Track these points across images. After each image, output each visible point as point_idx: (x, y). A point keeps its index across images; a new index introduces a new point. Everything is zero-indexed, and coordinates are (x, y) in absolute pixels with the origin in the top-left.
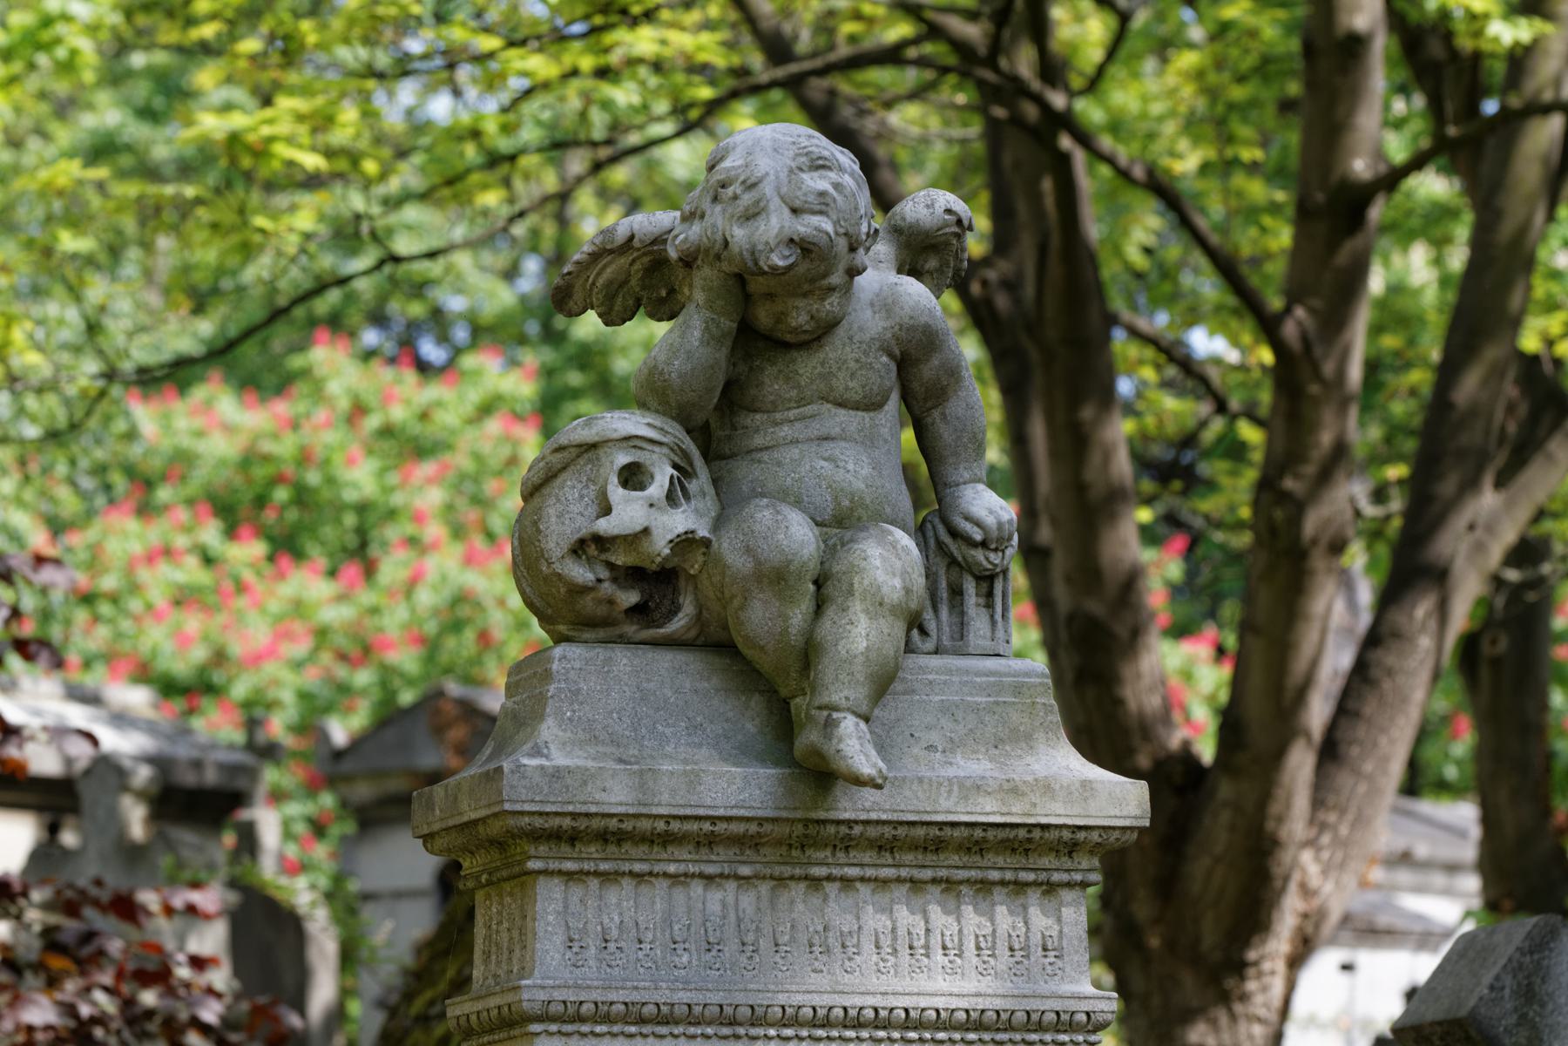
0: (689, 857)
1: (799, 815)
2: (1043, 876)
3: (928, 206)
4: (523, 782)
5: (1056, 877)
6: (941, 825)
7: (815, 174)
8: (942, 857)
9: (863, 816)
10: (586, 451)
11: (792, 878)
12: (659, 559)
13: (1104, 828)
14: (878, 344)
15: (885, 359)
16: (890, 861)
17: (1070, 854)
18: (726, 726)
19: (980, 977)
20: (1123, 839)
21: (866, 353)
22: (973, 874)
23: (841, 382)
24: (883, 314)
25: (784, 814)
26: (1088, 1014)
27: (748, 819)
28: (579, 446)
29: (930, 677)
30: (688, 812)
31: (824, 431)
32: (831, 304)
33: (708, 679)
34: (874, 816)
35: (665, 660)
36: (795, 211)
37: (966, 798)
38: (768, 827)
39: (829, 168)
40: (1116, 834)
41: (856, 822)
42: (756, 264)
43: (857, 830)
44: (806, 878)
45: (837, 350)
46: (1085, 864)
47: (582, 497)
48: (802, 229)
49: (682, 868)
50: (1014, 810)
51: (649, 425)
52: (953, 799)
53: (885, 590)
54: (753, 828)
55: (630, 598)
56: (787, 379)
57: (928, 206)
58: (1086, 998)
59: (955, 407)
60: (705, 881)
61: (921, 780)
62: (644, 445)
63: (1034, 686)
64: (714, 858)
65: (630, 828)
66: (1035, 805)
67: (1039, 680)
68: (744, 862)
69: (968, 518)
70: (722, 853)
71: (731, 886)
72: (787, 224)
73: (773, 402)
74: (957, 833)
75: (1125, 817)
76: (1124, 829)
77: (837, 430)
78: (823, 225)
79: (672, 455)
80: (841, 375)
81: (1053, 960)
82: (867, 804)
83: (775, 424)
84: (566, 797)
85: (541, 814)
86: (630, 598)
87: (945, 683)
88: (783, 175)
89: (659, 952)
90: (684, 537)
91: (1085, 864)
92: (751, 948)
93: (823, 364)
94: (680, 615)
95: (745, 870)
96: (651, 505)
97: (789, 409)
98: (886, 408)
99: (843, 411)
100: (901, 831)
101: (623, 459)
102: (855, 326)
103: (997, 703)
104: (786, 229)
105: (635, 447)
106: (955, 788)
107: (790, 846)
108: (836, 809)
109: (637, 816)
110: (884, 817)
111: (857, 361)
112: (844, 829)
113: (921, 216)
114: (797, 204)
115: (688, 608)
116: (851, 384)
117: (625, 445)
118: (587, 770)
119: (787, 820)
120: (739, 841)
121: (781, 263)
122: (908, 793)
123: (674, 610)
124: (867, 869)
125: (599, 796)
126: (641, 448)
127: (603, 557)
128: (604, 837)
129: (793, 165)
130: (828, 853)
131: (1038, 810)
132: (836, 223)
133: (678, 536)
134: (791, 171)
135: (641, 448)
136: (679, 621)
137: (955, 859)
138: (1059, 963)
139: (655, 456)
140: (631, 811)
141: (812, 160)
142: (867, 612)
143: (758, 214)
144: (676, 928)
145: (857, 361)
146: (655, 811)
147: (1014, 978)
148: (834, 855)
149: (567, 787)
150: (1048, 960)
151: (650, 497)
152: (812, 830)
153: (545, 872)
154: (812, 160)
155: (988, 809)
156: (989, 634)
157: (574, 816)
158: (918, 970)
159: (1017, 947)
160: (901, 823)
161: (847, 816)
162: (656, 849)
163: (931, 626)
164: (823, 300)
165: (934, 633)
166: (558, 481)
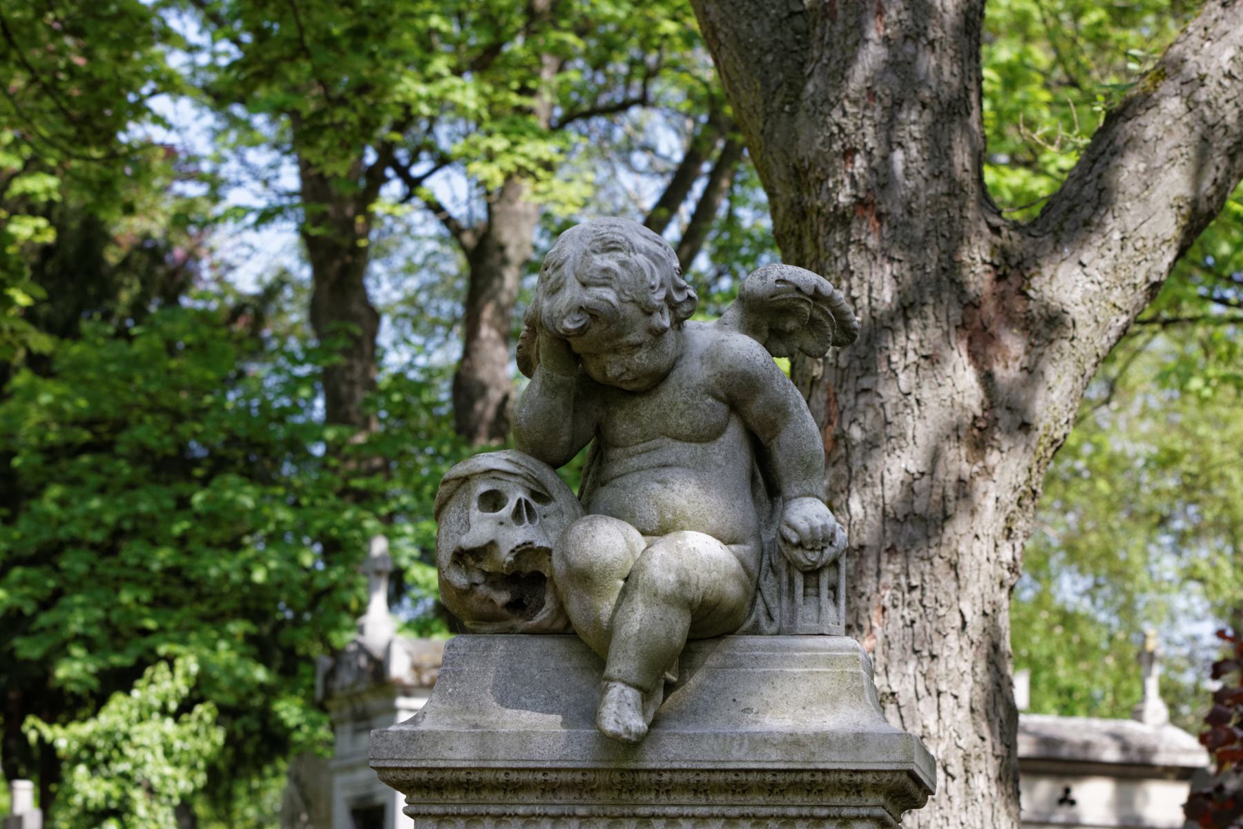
0: (536, 801)
1: (613, 765)
2: (834, 812)
3: (761, 278)
4: (385, 744)
5: (845, 812)
6: (737, 771)
7: (606, 255)
8: (749, 797)
9: (667, 766)
10: (463, 483)
11: (623, 816)
13: (877, 771)
14: (703, 389)
15: (710, 400)
16: (704, 801)
17: (859, 792)
18: (578, 696)
20: (895, 780)
21: (692, 397)
22: (775, 810)
23: (673, 420)
24: (709, 365)
25: (601, 765)
27: (574, 770)
28: (457, 479)
29: (757, 653)
30: (521, 765)
31: (663, 460)
32: (640, 358)
33: (570, 660)
34: (676, 765)
35: (537, 645)
36: (584, 285)
37: (755, 749)
38: (590, 777)
39: (620, 250)
40: (888, 776)
41: (665, 771)
42: (554, 325)
43: (666, 777)
44: (635, 816)
45: (670, 395)
46: (871, 801)
47: (459, 519)
48: (587, 299)
49: (529, 810)
50: (795, 758)
51: (507, 460)
52: (744, 750)
53: (659, 583)
54: (578, 777)
55: (502, 598)
56: (632, 420)
57: (761, 278)
59: (786, 437)
61: (716, 736)
62: (501, 476)
63: (846, 658)
64: (556, 801)
65: (477, 779)
66: (813, 754)
67: (849, 653)
68: (582, 805)
69: (789, 525)
70: (564, 797)
72: (577, 295)
73: (624, 439)
74: (751, 778)
75: (892, 763)
76: (893, 771)
77: (673, 458)
78: (604, 295)
79: (527, 484)
80: (673, 415)
82: (670, 756)
83: (630, 456)
84: (419, 755)
85: (403, 769)
86: (502, 598)
87: (769, 657)
88: (579, 258)
91: (871, 801)
93: (659, 406)
95: (581, 811)
96: (501, 523)
97: (637, 444)
98: (721, 439)
99: (678, 444)
100: (703, 777)
101: (483, 487)
102: (685, 375)
103: (811, 673)
104: (576, 300)
106: (746, 741)
107: (620, 791)
108: (644, 760)
109: (482, 769)
110: (685, 766)
111: (685, 403)
112: (654, 777)
113: (755, 286)
114: (585, 278)
115: (549, 603)
116: (681, 422)
118: (437, 733)
119: (607, 770)
120: (571, 787)
121: (571, 326)
122: (705, 746)
123: (542, 604)
125: (450, 754)
127: (478, 566)
128: (495, 787)
129: (588, 249)
130: (653, 795)
131: (817, 758)
132: (620, 292)
134: (586, 254)
137: (760, 799)
139: (510, 485)
140: (473, 765)
141: (605, 244)
142: (644, 601)
143: (558, 289)
145: (685, 403)
146: (493, 765)
148: (657, 795)
149: (421, 748)
151: (500, 517)
152: (628, 778)
154: (605, 244)
155: (774, 757)
156: (815, 618)
157: (430, 770)
160: (703, 771)
161: (653, 766)
162: (509, 795)
163: (776, 613)
164: (632, 355)
165: (777, 619)
166: (447, 508)
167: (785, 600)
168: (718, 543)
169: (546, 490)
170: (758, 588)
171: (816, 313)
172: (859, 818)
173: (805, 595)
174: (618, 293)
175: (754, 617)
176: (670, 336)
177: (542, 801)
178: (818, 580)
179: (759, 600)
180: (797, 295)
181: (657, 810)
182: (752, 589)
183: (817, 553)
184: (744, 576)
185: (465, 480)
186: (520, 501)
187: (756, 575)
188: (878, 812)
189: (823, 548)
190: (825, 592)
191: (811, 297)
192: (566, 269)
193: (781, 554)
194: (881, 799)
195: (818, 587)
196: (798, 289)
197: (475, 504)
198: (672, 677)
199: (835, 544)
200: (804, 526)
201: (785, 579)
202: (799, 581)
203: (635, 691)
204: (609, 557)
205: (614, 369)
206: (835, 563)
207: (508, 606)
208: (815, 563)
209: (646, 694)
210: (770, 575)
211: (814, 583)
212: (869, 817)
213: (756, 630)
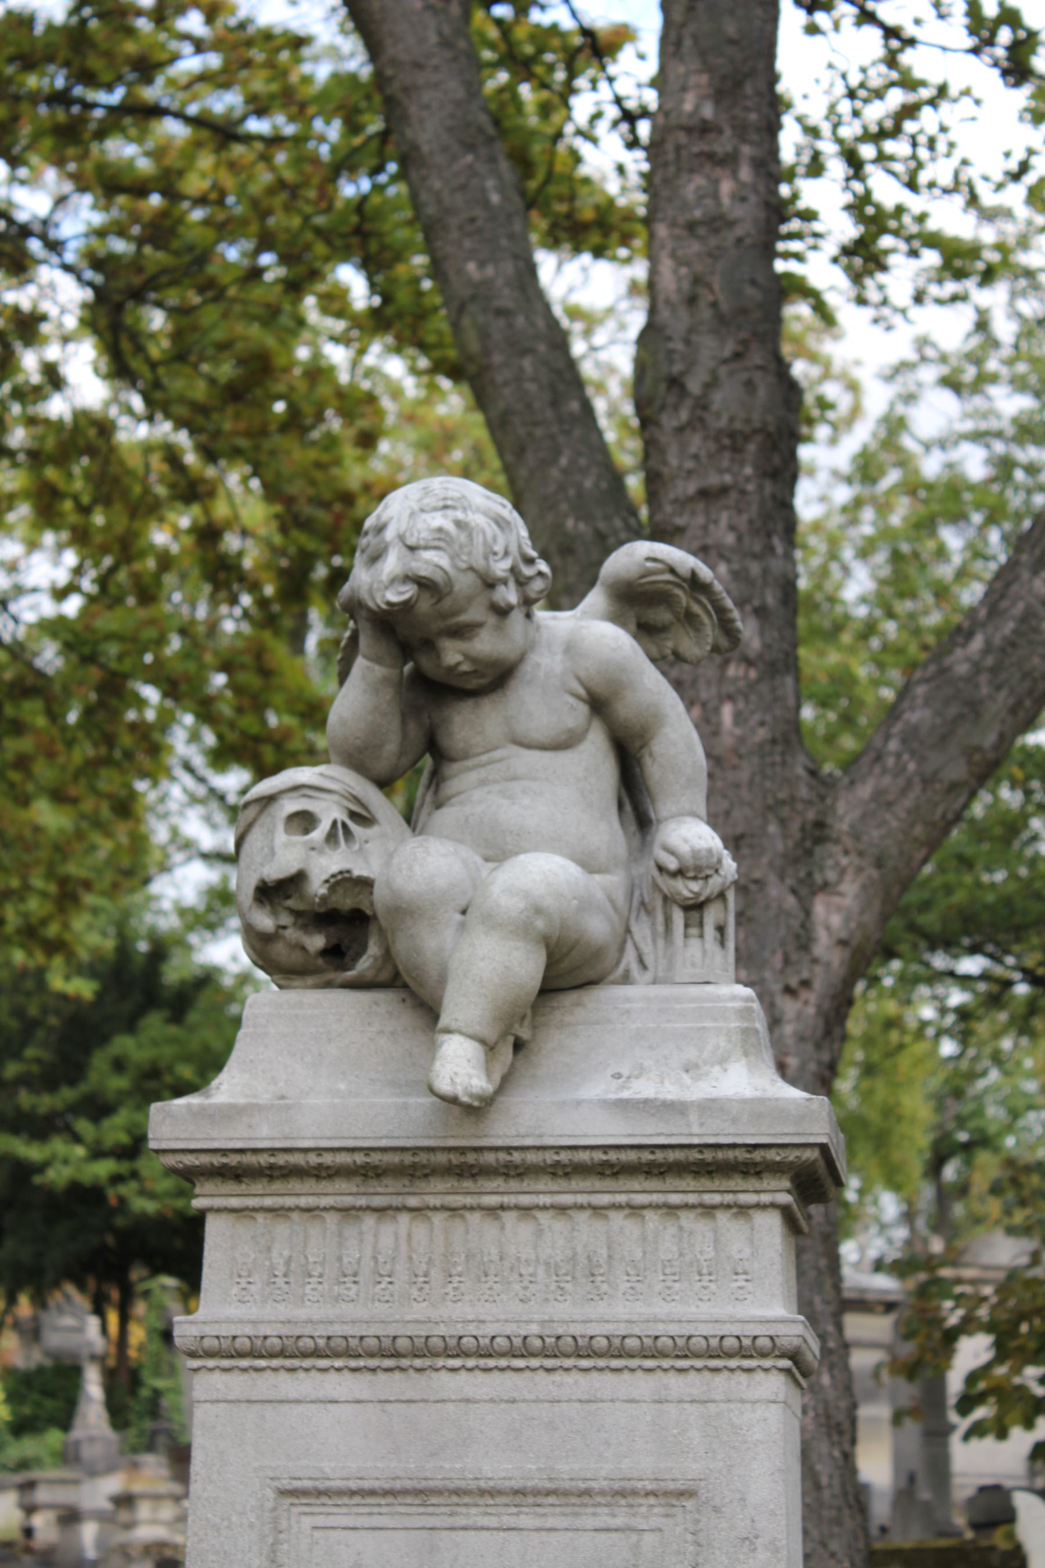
12: (317, 900)
19: (663, 1303)
26: (771, 1338)
27: (403, 1149)
29: (627, 1006)
39: (454, 508)
54: (408, 1159)
55: (317, 942)
58: (768, 1321)
60: (376, 1215)
71: (404, 1218)
81: (744, 1284)
86: (317, 942)
89: (326, 1286)
90: (339, 877)
92: (422, 1279)
94: (365, 957)
96: (313, 849)
101: (291, 805)
105: (304, 796)
112: (503, 1156)
114: (411, 541)
115: (373, 949)
117: (294, 794)
124: (541, 1196)
126: (309, 797)
133: (333, 876)
134: (412, 514)
138: (713, 1286)
144: (345, 1260)
147: (700, 1303)
151: (311, 841)
153: (219, 1210)
158: (597, 1298)
159: (705, 1271)
161: (499, 1142)
163: (649, 960)
167: (661, 943)
168: (579, 869)
170: (628, 931)
171: (696, 608)
172: (759, 1206)
173: (686, 936)
174: (452, 558)
176: (517, 617)
177: (362, 1190)
179: (629, 945)
180: (668, 577)
181: (506, 1199)
182: (621, 930)
183: (701, 882)
184: (611, 912)
185: (269, 800)
186: (334, 823)
187: (626, 912)
188: (785, 1198)
189: (707, 877)
190: (710, 931)
191: (684, 580)
192: (389, 534)
193: (656, 887)
195: (701, 925)
196: (672, 571)
197: (280, 827)
198: (525, 1033)
199: (722, 872)
200: (684, 849)
201: (660, 918)
202: (678, 917)
203: (476, 1044)
205: (452, 653)
206: (722, 896)
207: (325, 953)
208: (697, 894)
209: (490, 1048)
210: (643, 913)
212: (773, 1205)
213: (626, 979)
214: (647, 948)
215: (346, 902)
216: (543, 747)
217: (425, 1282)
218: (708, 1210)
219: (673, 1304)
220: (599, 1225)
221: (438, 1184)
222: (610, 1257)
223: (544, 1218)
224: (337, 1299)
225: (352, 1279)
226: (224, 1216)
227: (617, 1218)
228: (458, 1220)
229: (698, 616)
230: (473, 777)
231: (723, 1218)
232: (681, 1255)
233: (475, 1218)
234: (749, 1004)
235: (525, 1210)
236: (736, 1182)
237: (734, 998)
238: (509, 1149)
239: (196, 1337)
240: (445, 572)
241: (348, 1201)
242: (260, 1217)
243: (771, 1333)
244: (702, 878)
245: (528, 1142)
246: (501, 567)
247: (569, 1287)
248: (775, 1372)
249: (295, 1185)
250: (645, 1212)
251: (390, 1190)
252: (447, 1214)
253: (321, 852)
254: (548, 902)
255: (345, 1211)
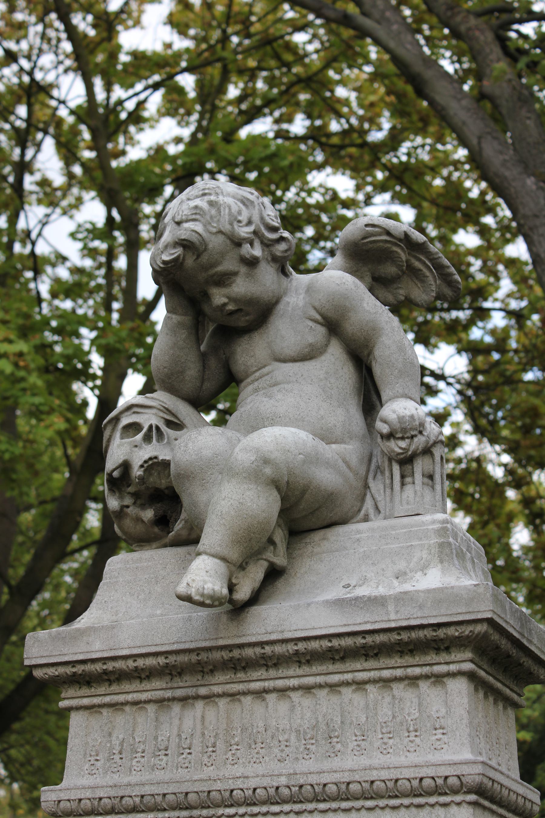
29: (358, 536)
39: (210, 194)
55: (149, 514)
60: (181, 704)
68: (201, 685)
71: (200, 705)
79: (162, 414)
81: (441, 736)
86: (149, 514)
90: (150, 462)
92: (211, 749)
96: (136, 446)
105: (134, 413)
126: (138, 413)
133: (146, 462)
135: (142, 413)
136: (178, 525)
144: (160, 739)
147: (408, 754)
150: (437, 737)
151: (134, 441)
158: (333, 755)
159: (411, 729)
161: (253, 639)
163: (381, 506)
169: (179, 419)
170: (366, 486)
171: (417, 264)
173: (403, 484)
174: (205, 226)
175: (364, 509)
177: (169, 685)
178: (413, 468)
179: (368, 496)
181: (266, 684)
183: (407, 441)
186: (151, 427)
188: (468, 666)
189: (412, 437)
191: (400, 240)
194: (469, 655)
196: (388, 233)
198: (280, 560)
199: (425, 433)
201: (387, 473)
202: (396, 469)
203: (217, 561)
204: (207, 453)
208: (406, 450)
211: (410, 471)
214: (379, 498)
215: (155, 481)
216: (294, 360)
217: (213, 751)
218: (413, 681)
219: (389, 756)
220: (335, 699)
221: (220, 677)
222: (342, 722)
223: (295, 696)
224: (153, 768)
225: (164, 752)
226: (81, 712)
227: (347, 692)
228: (237, 703)
229: (421, 270)
230: (250, 388)
231: (424, 685)
232: (394, 717)
233: (247, 700)
234: (445, 525)
235: (283, 691)
236: (431, 658)
237: (434, 522)
238: (262, 644)
239: (55, 801)
240: (200, 235)
241: (159, 694)
242: (105, 711)
243: (458, 773)
244: (408, 438)
245: (274, 637)
246: (244, 231)
247: (313, 748)
248: (464, 804)
249: (126, 686)
250: (367, 686)
251: (187, 684)
252: (228, 699)
253: (141, 448)
254: (275, 455)
255: (160, 702)
